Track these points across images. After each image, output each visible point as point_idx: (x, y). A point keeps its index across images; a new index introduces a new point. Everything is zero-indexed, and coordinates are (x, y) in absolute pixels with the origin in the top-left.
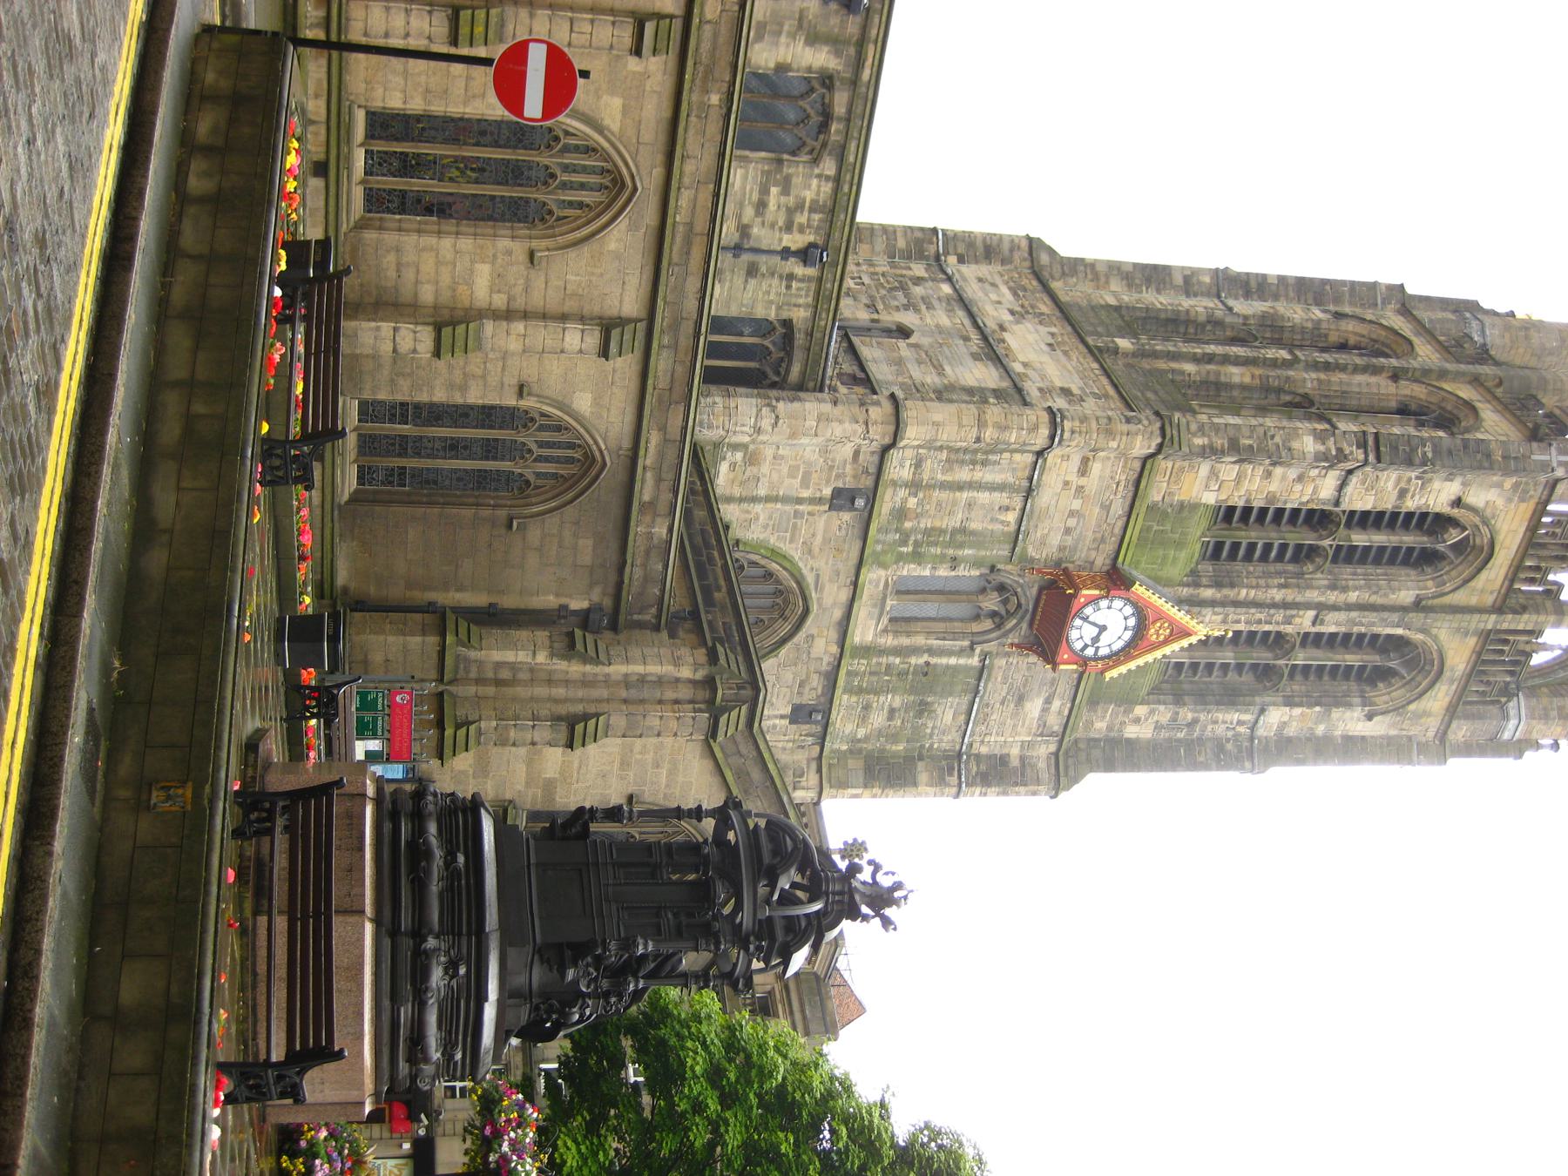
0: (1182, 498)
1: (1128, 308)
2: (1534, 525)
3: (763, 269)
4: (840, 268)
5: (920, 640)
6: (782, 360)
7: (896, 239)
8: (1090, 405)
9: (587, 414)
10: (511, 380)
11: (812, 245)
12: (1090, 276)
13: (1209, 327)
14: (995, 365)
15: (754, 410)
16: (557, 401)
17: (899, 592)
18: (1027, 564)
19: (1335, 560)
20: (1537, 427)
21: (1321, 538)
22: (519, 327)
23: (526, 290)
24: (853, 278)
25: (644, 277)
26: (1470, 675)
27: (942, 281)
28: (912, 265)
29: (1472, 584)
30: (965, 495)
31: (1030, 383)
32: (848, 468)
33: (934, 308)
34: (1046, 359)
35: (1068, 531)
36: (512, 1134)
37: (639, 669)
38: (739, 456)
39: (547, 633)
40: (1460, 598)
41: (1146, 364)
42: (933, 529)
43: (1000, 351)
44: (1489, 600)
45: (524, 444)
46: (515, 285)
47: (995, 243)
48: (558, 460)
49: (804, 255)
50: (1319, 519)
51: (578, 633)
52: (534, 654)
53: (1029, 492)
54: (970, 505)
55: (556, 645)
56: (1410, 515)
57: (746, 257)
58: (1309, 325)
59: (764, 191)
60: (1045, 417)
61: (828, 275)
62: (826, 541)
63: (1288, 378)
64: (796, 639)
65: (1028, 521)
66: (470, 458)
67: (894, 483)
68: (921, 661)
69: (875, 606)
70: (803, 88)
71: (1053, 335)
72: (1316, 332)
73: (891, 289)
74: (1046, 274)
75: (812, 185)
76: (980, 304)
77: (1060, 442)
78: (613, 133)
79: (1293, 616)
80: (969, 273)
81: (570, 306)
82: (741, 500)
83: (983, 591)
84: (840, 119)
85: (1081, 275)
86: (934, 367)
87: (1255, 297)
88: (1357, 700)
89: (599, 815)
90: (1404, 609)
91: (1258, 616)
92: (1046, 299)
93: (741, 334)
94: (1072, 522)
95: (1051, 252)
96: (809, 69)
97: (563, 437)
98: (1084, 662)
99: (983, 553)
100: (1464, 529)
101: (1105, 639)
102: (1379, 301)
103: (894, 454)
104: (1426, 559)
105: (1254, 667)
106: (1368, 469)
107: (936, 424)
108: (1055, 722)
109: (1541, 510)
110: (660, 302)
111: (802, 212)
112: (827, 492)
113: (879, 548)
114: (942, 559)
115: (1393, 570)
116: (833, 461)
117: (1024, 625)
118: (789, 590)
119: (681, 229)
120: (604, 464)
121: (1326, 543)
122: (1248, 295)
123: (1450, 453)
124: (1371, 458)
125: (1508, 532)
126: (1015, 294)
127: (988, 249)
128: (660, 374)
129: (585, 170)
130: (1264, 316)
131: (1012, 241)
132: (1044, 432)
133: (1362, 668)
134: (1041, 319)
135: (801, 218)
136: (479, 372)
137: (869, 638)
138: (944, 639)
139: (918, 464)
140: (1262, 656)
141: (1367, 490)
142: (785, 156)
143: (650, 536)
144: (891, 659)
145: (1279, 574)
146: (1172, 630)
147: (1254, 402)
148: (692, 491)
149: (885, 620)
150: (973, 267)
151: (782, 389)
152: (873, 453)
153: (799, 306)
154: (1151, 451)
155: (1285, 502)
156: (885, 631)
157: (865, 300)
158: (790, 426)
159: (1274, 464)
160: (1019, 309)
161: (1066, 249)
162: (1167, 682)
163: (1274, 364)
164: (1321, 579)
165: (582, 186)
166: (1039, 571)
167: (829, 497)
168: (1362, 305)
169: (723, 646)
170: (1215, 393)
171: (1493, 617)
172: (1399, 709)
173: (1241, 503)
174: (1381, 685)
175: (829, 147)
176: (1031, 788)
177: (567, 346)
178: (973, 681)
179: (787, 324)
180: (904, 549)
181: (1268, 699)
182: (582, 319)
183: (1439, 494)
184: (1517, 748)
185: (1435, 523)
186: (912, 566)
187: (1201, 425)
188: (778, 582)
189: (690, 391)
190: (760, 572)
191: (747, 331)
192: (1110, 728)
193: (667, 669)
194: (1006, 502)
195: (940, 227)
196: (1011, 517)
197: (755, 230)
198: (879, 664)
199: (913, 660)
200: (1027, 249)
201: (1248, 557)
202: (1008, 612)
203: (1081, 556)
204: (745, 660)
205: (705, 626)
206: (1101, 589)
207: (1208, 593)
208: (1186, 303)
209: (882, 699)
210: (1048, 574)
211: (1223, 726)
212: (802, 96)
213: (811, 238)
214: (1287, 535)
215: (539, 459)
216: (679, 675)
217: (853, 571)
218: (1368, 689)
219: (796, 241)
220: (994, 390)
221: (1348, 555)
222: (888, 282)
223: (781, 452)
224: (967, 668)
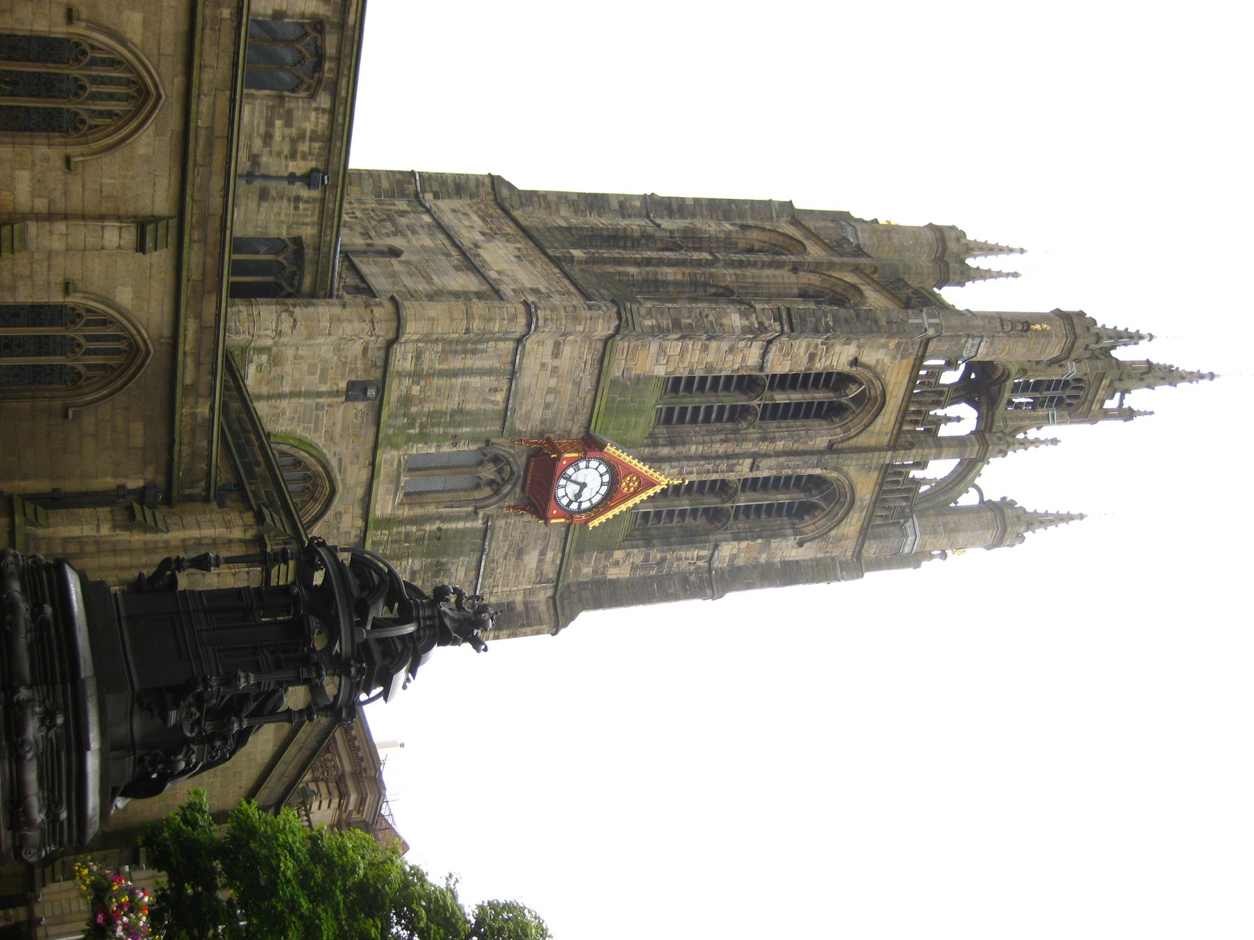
0: (639, 372)
1: (576, 228)
2: (914, 376)
3: (273, 193)
4: (339, 189)
5: (432, 509)
6: (294, 273)
7: (381, 182)
8: (556, 300)
9: (129, 307)
10: (57, 279)
11: (314, 170)
12: (543, 205)
13: (643, 241)
14: (473, 273)
15: (275, 316)
16: (101, 296)
17: (410, 470)
18: (516, 436)
19: (762, 418)
20: (909, 299)
21: (751, 399)
22: (61, 227)
23: (65, 193)
24: (347, 214)
25: (173, 178)
26: (875, 503)
27: (422, 213)
28: (396, 202)
29: (871, 428)
30: (460, 380)
31: (505, 286)
32: (359, 364)
33: (418, 233)
34: (515, 267)
35: (547, 406)
36: (125, 919)
37: (195, 533)
38: (264, 358)
39: (108, 509)
40: (862, 440)
41: (597, 269)
42: (435, 412)
43: (477, 263)
44: (885, 440)
45: (74, 339)
46: (54, 190)
47: (463, 181)
48: (105, 352)
49: (309, 179)
50: (747, 383)
51: (136, 506)
52: (98, 527)
53: (513, 375)
54: (464, 389)
55: (118, 518)
56: (818, 375)
57: (257, 183)
58: (722, 235)
59: (270, 124)
60: (522, 309)
61: (329, 196)
62: (345, 429)
63: (711, 274)
64: (326, 517)
65: (514, 401)
66: (24, 354)
67: (399, 374)
68: (434, 527)
69: (391, 482)
70: (298, 33)
71: (519, 249)
72: (728, 241)
73: (381, 220)
74: (507, 205)
75: (311, 119)
76: (456, 229)
77: (536, 328)
78: (135, 45)
79: (734, 465)
80: (445, 207)
81: (106, 207)
82: (269, 397)
83: (481, 463)
84: (331, 59)
85: (536, 205)
86: (424, 277)
87: (677, 216)
88: (789, 531)
89: (185, 564)
90: (821, 453)
91: (707, 466)
92: (510, 223)
93: (257, 253)
94: (550, 398)
95: (510, 187)
96: (303, 16)
97: (109, 331)
98: (570, 515)
99: (478, 430)
100: (861, 384)
101: (586, 494)
102: (774, 215)
103: (398, 349)
104: (832, 412)
105: (706, 511)
106: (784, 338)
107: (432, 319)
108: (550, 571)
109: (918, 365)
110: (188, 199)
111: (304, 142)
112: (343, 385)
113: (391, 431)
114: (445, 437)
115: (809, 422)
116: (346, 357)
117: (518, 490)
118: (317, 475)
119: (202, 133)
120: (148, 353)
121: (755, 403)
122: (671, 214)
123: (846, 321)
124: (786, 328)
125: (895, 383)
126: (484, 220)
127: (457, 186)
128: (193, 266)
129: (111, 81)
130: (686, 230)
131: (478, 179)
132: (522, 320)
133: (791, 505)
134: (507, 238)
135: (304, 147)
136: (27, 272)
137: (389, 511)
138: (452, 507)
139: (418, 357)
140: (712, 501)
141: (784, 356)
142: (286, 93)
143: (194, 416)
144: (409, 528)
145: (720, 431)
146: (640, 483)
147: (687, 295)
148: (226, 388)
149: (400, 495)
150: (447, 201)
151: (297, 297)
152: (379, 349)
153: (307, 224)
154: (611, 332)
155: (721, 370)
156: (401, 504)
157: (359, 229)
158: (306, 327)
159: (710, 338)
160: (488, 231)
161: (522, 184)
162: (637, 530)
163: (699, 263)
164: (754, 433)
165: (111, 97)
166: (527, 442)
167: (345, 389)
168: (761, 219)
169: (268, 509)
170: (654, 288)
171: (890, 453)
172: (822, 536)
173: (686, 374)
174: (807, 518)
175: (323, 84)
176: (536, 628)
177: (106, 243)
178: (479, 541)
179: (297, 241)
180: (412, 431)
181: (719, 537)
182: (119, 218)
183: (839, 357)
184: (914, 560)
185: (838, 381)
186: (420, 445)
187: (647, 314)
188: (307, 468)
189: (221, 281)
190: (289, 460)
191: (263, 249)
192: (595, 572)
193: (220, 532)
194: (495, 384)
195: (417, 169)
196: (500, 397)
197: (264, 159)
198: (399, 533)
199: (428, 527)
200: (490, 185)
201: (694, 420)
202: (503, 479)
203: (560, 426)
204: (288, 519)
205: (250, 494)
206: (579, 452)
207: (665, 451)
208: (623, 223)
209: (404, 563)
210: (536, 443)
211: (686, 562)
212: (298, 40)
213: (313, 164)
214: (724, 399)
215: (88, 352)
216: (231, 536)
217: (370, 453)
218: (797, 521)
219: (299, 167)
220: (476, 293)
221: (775, 413)
222: (377, 215)
223: (300, 352)
224: (473, 530)
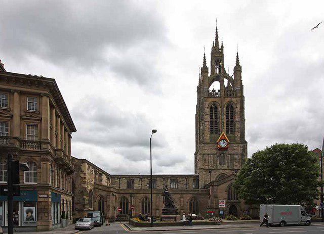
50: (211, 122)
104: (216, 108)
114: (217, 162)
183: (207, 110)
184: (242, 86)
